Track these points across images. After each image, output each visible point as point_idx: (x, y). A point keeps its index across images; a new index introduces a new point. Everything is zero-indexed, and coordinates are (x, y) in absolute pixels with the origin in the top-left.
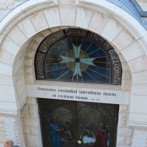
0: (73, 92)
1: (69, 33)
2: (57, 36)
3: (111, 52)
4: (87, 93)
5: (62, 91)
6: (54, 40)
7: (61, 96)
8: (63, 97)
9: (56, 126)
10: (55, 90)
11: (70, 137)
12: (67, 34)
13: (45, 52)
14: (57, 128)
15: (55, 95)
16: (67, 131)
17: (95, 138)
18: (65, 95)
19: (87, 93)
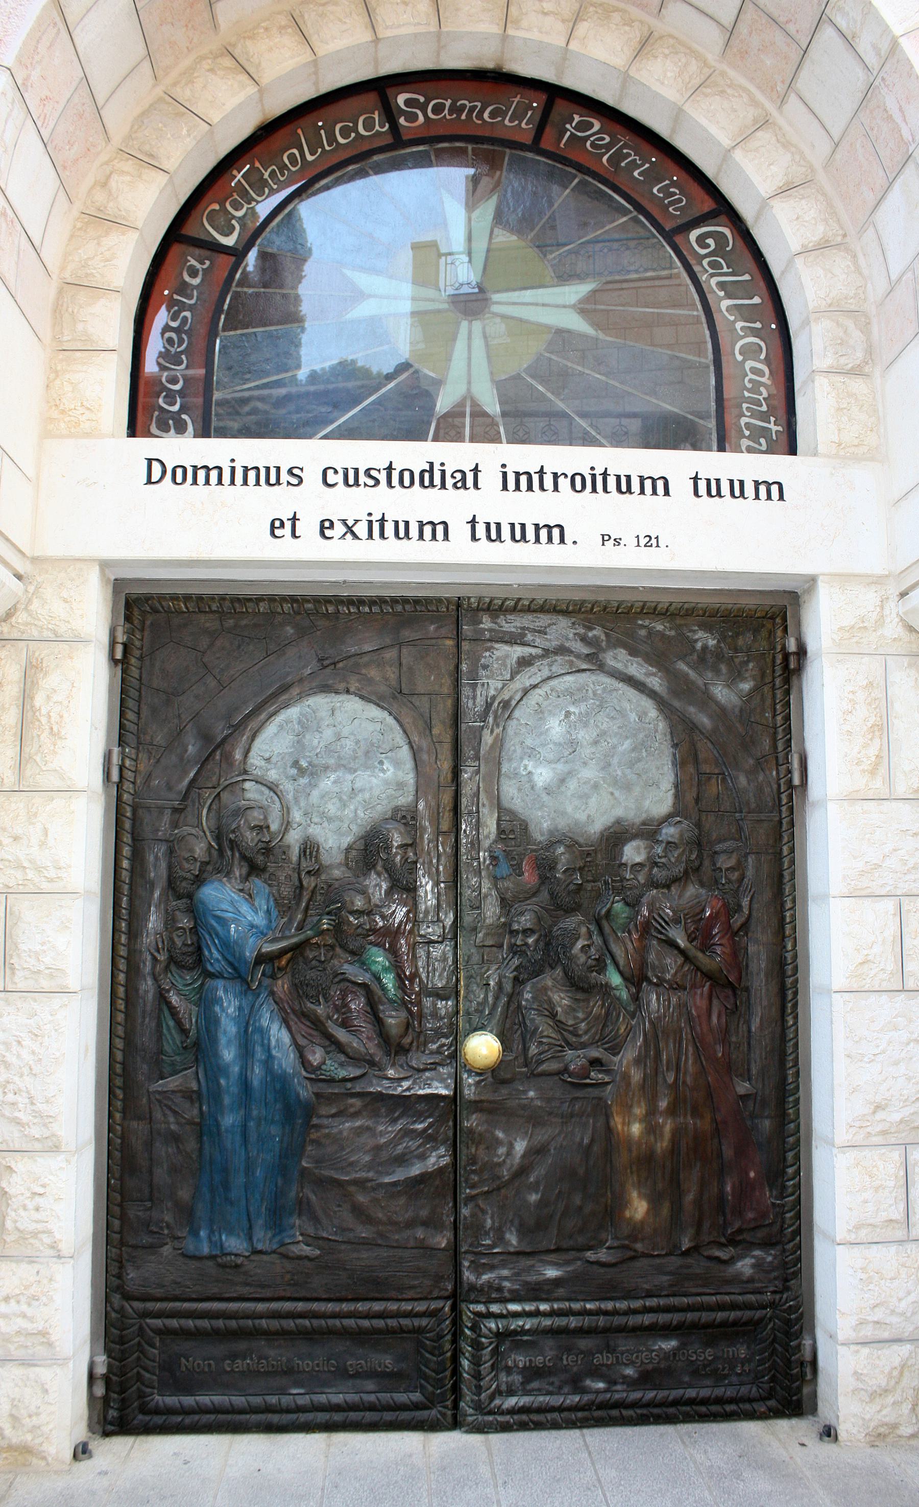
0: (443, 486)
1: (421, 118)
2: (332, 139)
3: (701, 240)
4: (564, 483)
5: (351, 479)
6: (310, 158)
7: (340, 529)
8: (361, 530)
10: (296, 476)
12: (402, 121)
13: (229, 241)
15: (294, 519)
18: (376, 516)
19: (564, 483)
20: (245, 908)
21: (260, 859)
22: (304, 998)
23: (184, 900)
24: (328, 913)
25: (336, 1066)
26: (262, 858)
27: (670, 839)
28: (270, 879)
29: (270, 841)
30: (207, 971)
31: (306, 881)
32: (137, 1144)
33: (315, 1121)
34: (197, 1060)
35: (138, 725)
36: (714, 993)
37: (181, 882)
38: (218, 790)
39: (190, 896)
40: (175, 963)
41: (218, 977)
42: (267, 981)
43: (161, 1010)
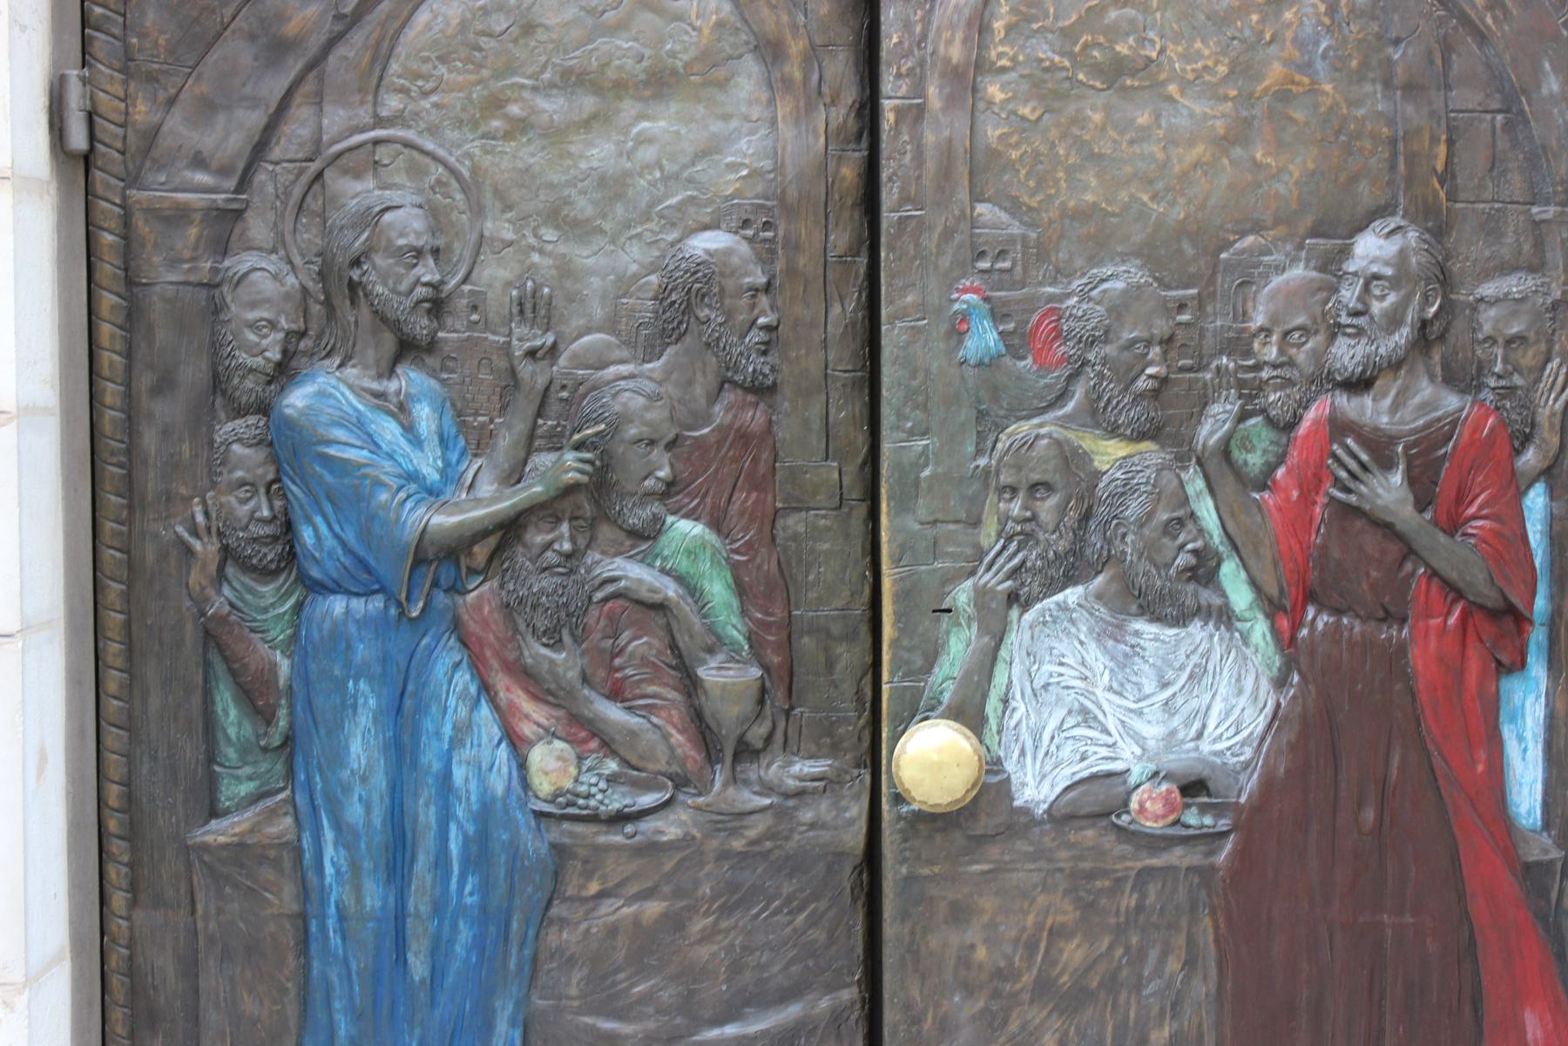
9: (424, 416)
11: (711, 673)
14: (428, 465)
16: (645, 537)
17: (1260, 630)
20: (388, 430)
21: (421, 326)
22: (529, 638)
23: (252, 420)
24: (578, 447)
25: (602, 785)
26: (425, 322)
27: (1375, 269)
28: (443, 368)
29: (442, 282)
30: (310, 578)
31: (526, 369)
32: (163, 963)
33: (554, 911)
34: (290, 774)
35: (124, 15)
36: (1471, 629)
37: (243, 377)
38: (314, 167)
39: (264, 408)
40: (236, 560)
41: (334, 592)
42: (441, 599)
43: (207, 665)
